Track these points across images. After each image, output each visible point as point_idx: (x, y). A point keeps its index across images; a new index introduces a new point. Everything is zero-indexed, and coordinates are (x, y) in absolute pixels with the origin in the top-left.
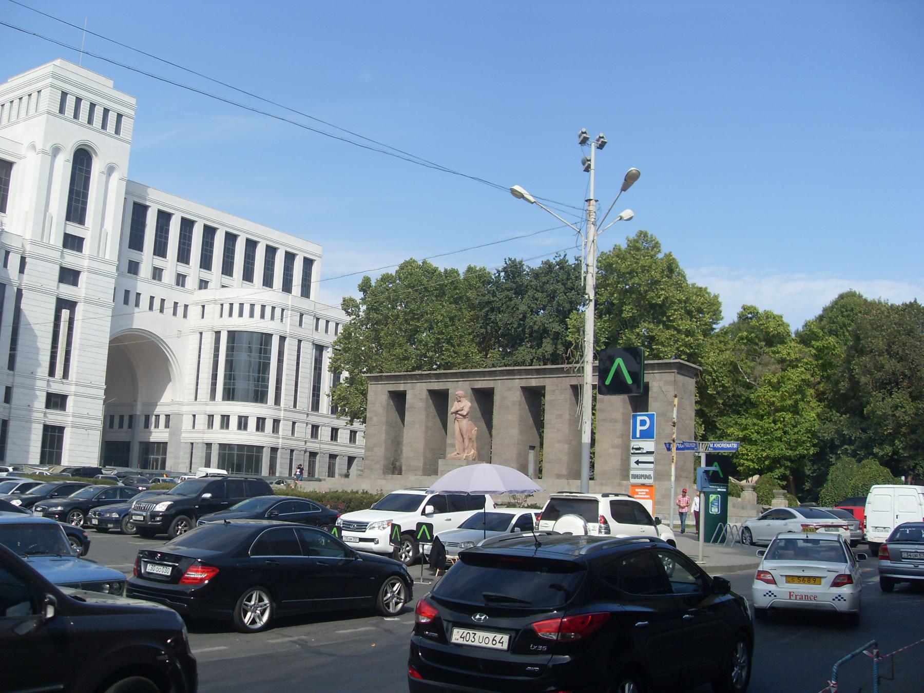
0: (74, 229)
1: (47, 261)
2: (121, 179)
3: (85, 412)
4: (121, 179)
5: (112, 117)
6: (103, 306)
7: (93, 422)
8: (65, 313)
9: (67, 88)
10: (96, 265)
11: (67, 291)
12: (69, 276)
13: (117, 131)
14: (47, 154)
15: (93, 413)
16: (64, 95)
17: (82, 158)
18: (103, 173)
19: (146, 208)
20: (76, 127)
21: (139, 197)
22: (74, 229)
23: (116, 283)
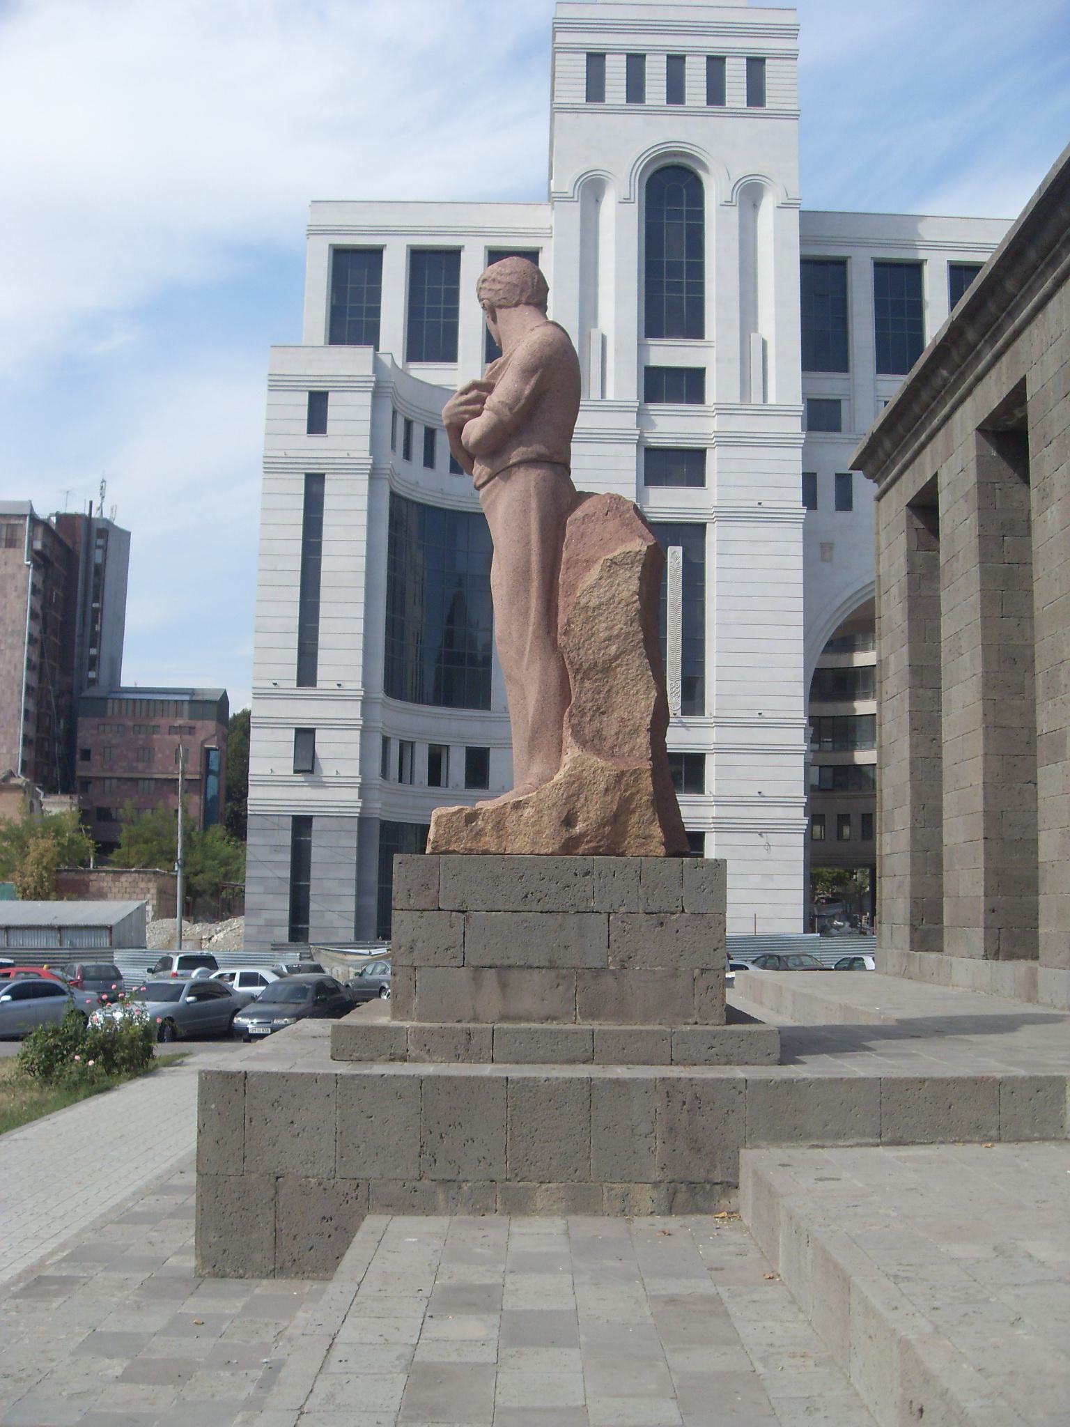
0: (670, 353)
1: (602, 441)
2: (784, 206)
3: (751, 790)
4: (784, 206)
5: (735, 73)
6: (772, 520)
7: (779, 812)
8: (675, 556)
9: (597, 41)
10: (738, 425)
11: (668, 502)
12: (675, 465)
13: (756, 95)
14: (569, 200)
15: (770, 791)
16: (596, 60)
17: (671, 193)
18: (728, 204)
19: (916, 268)
20: (639, 119)
21: (889, 246)
22: (670, 353)
23: (804, 454)
